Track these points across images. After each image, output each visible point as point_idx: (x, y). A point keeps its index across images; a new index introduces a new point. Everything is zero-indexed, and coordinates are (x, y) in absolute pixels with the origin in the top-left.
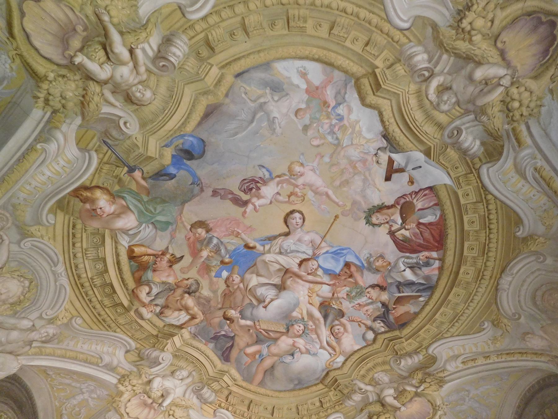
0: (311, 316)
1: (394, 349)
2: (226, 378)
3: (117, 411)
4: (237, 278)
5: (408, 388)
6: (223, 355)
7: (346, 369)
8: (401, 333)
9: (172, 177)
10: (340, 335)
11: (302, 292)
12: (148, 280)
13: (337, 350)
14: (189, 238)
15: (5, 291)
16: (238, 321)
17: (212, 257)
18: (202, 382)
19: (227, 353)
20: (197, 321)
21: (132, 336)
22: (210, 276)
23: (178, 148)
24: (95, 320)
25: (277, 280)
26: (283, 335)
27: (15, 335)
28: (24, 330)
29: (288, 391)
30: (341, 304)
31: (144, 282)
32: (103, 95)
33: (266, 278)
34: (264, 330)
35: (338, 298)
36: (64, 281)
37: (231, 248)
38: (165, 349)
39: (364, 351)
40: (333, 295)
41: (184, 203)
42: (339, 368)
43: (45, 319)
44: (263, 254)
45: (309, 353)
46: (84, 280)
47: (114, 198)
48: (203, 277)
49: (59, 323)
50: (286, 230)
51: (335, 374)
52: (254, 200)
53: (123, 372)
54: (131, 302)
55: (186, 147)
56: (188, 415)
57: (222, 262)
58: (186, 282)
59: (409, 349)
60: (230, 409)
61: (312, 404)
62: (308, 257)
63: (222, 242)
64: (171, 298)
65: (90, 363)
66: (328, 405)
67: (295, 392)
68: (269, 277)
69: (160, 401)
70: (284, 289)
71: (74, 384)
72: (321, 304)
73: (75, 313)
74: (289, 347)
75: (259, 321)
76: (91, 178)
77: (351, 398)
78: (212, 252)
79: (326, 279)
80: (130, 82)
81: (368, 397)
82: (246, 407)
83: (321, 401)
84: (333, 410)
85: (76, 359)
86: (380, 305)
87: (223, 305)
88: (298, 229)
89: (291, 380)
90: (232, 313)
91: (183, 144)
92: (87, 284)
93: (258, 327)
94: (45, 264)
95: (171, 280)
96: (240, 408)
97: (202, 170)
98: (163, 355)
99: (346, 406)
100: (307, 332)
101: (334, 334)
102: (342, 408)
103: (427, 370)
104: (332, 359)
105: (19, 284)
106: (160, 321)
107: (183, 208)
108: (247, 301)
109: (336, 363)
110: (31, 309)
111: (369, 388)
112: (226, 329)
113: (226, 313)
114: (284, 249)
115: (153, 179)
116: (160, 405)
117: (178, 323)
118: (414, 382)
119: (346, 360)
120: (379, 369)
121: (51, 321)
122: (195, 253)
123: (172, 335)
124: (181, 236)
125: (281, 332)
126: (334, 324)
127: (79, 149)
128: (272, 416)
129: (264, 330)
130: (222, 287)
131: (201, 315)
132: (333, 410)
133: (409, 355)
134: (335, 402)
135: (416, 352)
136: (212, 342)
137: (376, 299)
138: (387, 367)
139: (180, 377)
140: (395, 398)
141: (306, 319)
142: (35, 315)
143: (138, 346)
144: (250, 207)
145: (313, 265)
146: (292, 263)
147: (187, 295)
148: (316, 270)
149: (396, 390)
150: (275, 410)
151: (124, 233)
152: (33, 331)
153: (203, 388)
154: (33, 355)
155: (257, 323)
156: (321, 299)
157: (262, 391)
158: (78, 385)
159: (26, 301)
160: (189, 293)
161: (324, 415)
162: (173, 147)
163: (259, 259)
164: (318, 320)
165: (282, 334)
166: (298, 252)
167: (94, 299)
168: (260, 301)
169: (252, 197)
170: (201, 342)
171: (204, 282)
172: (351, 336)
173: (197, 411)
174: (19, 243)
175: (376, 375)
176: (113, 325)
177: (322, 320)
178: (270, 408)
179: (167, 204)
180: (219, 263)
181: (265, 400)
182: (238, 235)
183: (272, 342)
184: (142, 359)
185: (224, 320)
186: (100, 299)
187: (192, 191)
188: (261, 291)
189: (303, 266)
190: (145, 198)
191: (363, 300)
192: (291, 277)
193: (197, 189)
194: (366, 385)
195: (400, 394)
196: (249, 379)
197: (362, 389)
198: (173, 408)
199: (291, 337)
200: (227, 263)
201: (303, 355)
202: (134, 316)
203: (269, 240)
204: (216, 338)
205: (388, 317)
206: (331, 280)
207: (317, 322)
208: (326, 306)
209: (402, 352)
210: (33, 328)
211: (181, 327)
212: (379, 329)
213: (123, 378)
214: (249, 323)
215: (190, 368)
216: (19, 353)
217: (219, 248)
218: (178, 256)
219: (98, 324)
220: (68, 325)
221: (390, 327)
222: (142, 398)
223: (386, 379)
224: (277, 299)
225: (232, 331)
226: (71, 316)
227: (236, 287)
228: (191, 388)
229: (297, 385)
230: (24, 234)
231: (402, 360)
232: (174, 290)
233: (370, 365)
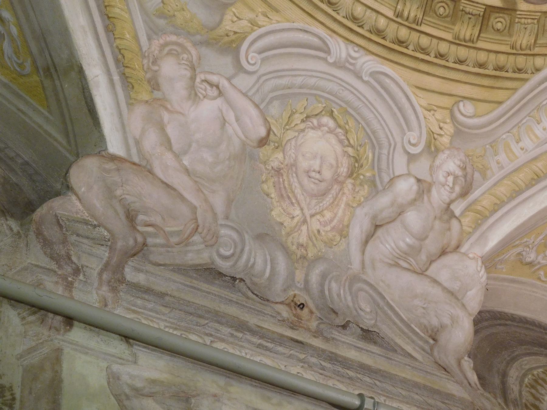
15: (318, 162)
27: (413, 218)
28: (415, 200)
36: (369, 63)
43: (420, 154)
46: (392, 30)
49: (446, 140)
73: (447, 102)
92: (403, 33)
94: (312, 65)
105: (320, 133)
110: (384, 157)
121: (432, 149)
142: (400, 164)
152: (429, 191)
154: (475, 229)
159: (361, 150)
167: (443, 47)
174: (239, 68)
176: (521, 61)
186: (449, 36)
202: (532, 7)
210: (424, 187)
216: (454, 243)
219: (499, 84)
220: (460, 132)
226: (447, 112)
230: (230, 46)
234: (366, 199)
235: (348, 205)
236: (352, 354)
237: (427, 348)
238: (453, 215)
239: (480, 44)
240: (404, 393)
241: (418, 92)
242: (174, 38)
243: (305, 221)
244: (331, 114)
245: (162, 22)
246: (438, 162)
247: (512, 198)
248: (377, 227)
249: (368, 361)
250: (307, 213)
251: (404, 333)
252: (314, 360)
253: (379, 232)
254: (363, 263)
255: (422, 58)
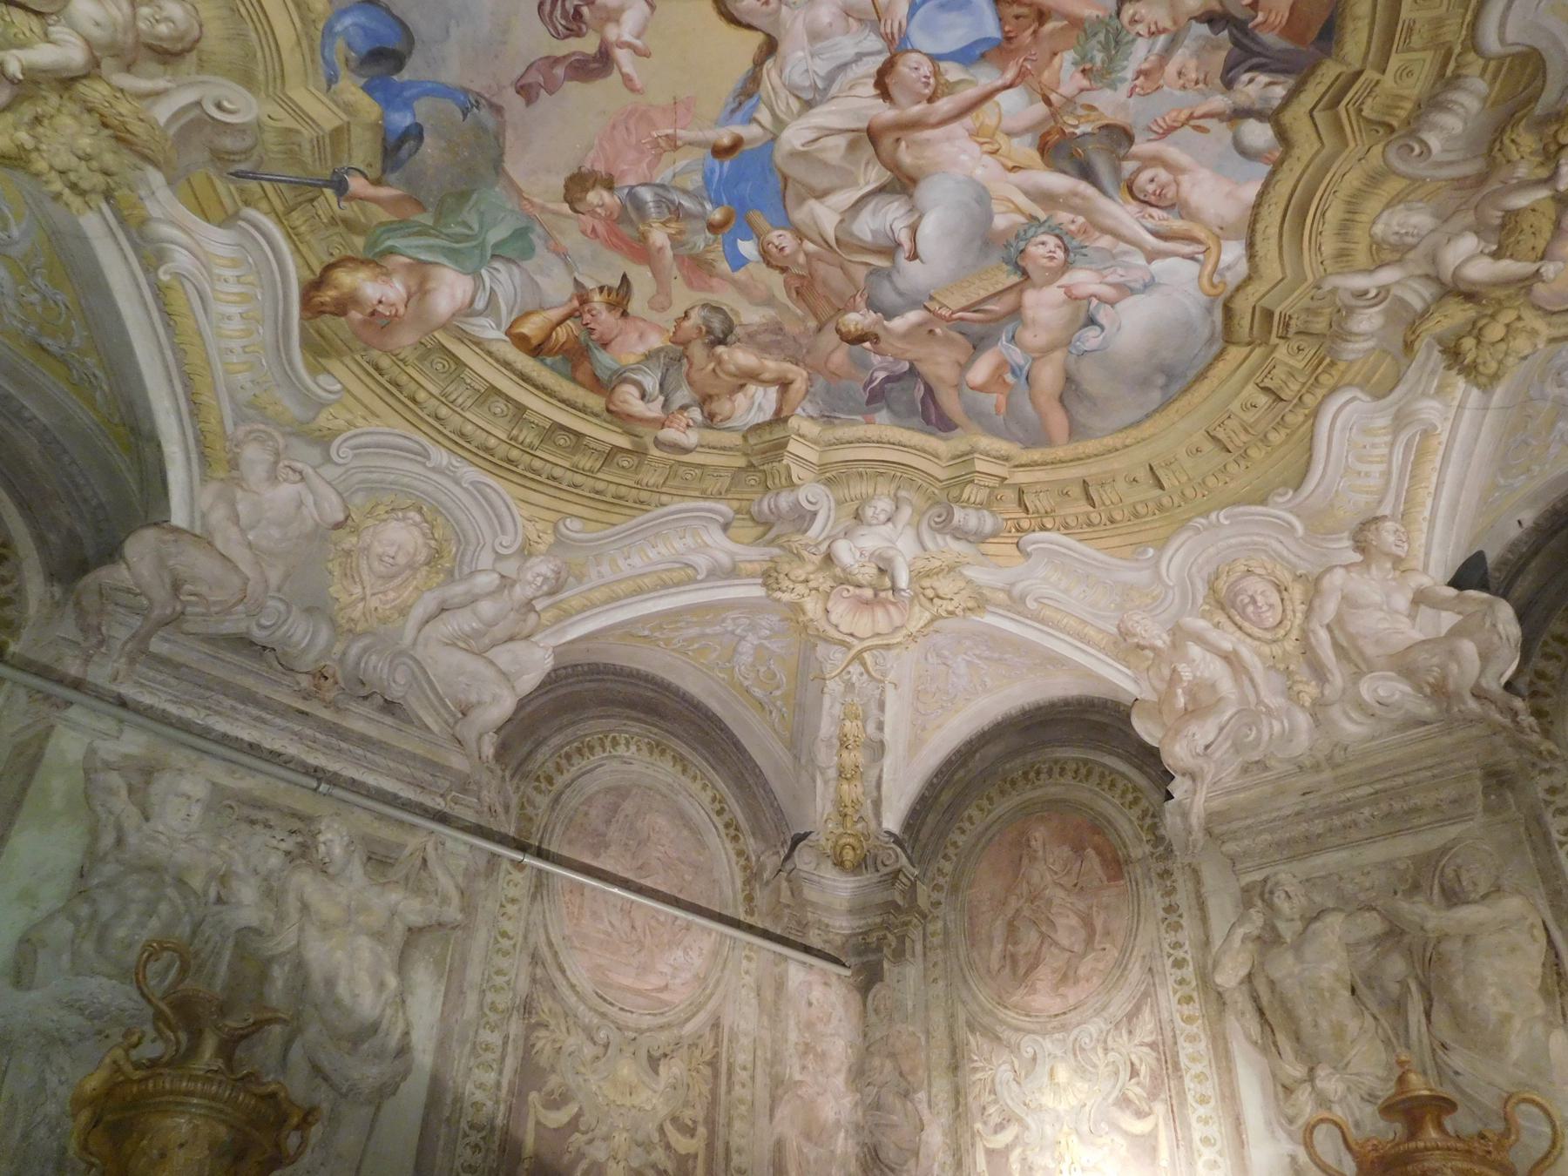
0: (1046, 198)
1: (1368, 121)
2: (980, 465)
3: (828, 640)
4: (782, 239)
5: (1521, 201)
6: (928, 422)
7: (1271, 269)
8: (1342, 61)
9: (415, 133)
10: (1170, 192)
11: (964, 157)
12: (615, 372)
13: (1200, 233)
14: (594, 230)
15: (394, 549)
16: (885, 328)
17: (680, 232)
18: (938, 503)
19: (932, 410)
20: (799, 385)
21: (704, 491)
22: (722, 277)
23: (353, 64)
24: (602, 506)
25: (874, 176)
26: (1022, 291)
27: (487, 608)
29: (1156, 411)
30: (1091, 108)
31: (610, 381)
32: (122, 90)
33: (842, 188)
34: (964, 309)
35: (1070, 101)
36: (470, 473)
37: (694, 181)
38: (795, 479)
39: (1283, 188)
40: (1048, 101)
41: (497, 165)
42: (1249, 279)
44: (775, 138)
45: (1133, 291)
47: (378, 265)
48: (711, 289)
49: (542, 547)
50: (756, 39)
51: (1252, 300)
52: (612, 32)
53: (758, 567)
54: (628, 433)
55: (364, 47)
56: (969, 582)
57: (713, 228)
58: (686, 324)
59: (1416, 87)
60: (1049, 526)
61: (1244, 408)
62: (880, 60)
63: (662, 186)
64: (695, 376)
65: (677, 585)
66: (1295, 387)
67: (1177, 405)
68: (849, 181)
69: (888, 583)
70: (914, 181)
71: (708, 631)
72: (1043, 149)
74: (1066, 311)
75: (932, 298)
76: (301, 261)
77: (1351, 333)
78: (669, 220)
79: (986, 77)
80: (120, 19)
81: (1401, 302)
82: (1083, 502)
83: (1266, 390)
84: (1320, 393)
85: (639, 591)
86: (1204, 29)
87: (816, 315)
88: (778, 11)
89: (1144, 383)
90: (855, 320)
91: (350, 46)
92: (515, 454)
93: (944, 312)
94: (407, 466)
95: (656, 341)
96: (1072, 511)
97: (445, 61)
98: (802, 495)
99: (1351, 363)
100: (1075, 243)
101: (1153, 199)
102: (1343, 373)
103: (1539, 109)
104: (1209, 268)
106: (726, 434)
107: (512, 182)
108: (860, 273)
109: (1228, 268)
110: (469, 553)
111: (1387, 276)
112: (879, 367)
113: (844, 329)
114: (803, 89)
115: (395, 168)
116: (894, 589)
117: (768, 414)
118: (1522, 171)
119: (1251, 245)
120: (1372, 205)
121: (526, 551)
122: (641, 251)
123: (781, 445)
124: (572, 236)
125: (1011, 288)
126: (1126, 174)
127: (219, 226)
128: (1162, 487)
129: (964, 309)
130: (775, 280)
131: (794, 367)
132: (1320, 393)
133: (1432, 103)
134: (1308, 370)
135: (1447, 80)
136: (877, 410)
137: (1175, 22)
138: (1394, 186)
139: (883, 517)
140: (1496, 255)
141: (1042, 216)
142: (486, 559)
143: (736, 504)
144: (622, 55)
145: (913, 68)
146: (859, 104)
147: (720, 349)
148: (936, 73)
149: (1479, 230)
150: (1160, 473)
151: (467, 316)
152: (512, 586)
153: (950, 514)
155: (934, 306)
156: (1028, 138)
157: (1091, 446)
158: (718, 629)
160: (722, 342)
161: (1301, 418)
162: (343, 72)
163: (779, 157)
164: (1076, 194)
165: (1018, 288)
166: (843, 67)
167: (557, 472)
168: (889, 250)
169: (600, 30)
170: (853, 423)
171: (727, 298)
172: (1204, 174)
173: (981, 564)
174: (328, 459)
175: (1379, 229)
176: (644, 495)
177: (1084, 187)
178: (1142, 474)
179: (475, 197)
180: (709, 235)
181: (1117, 463)
182: (673, 143)
183: (1010, 327)
184: (768, 525)
185: (856, 348)
186: (567, 465)
187: (480, 128)
188: (866, 226)
189: (894, 91)
190: (426, 219)
191: (1140, 53)
192: (898, 140)
193: (484, 114)
194: (1371, 272)
195: (1504, 235)
196: (1037, 437)
197: (1366, 292)
198: (926, 583)
199: (1049, 282)
200: (724, 224)
201: (1118, 306)
203: (750, 96)
204: (877, 397)
205: (1259, 43)
206: (1004, 70)
207: (1078, 201)
208: (1057, 146)
209: (1403, 114)
210: (506, 583)
211: (779, 419)
212: (1267, 100)
213: (769, 577)
214: (914, 316)
215: (884, 488)
216: (525, 633)
217: (672, 202)
218: (616, 283)
219: (616, 509)
220: (560, 542)
221: (1297, 69)
222: (845, 594)
223: (1420, 219)
224: (921, 217)
225: (897, 359)
227: (801, 259)
228: (924, 527)
229: (1165, 387)
230: (323, 440)
231: (1425, 136)
232: (684, 355)
233: (1334, 214)
234: (439, 585)
235: (416, 588)
236: (359, 726)
237: (451, 721)
238: (533, 609)
239: (599, 475)
240: (392, 765)
241: (522, 505)
242: (262, 427)
243: (363, 599)
244: (420, 510)
245: (251, 412)
246: (528, 564)
247: (606, 602)
248: (443, 610)
249: (373, 732)
250: (368, 592)
251: (432, 706)
252: (309, 732)
253: (445, 615)
254: (415, 643)
255: (531, 477)
